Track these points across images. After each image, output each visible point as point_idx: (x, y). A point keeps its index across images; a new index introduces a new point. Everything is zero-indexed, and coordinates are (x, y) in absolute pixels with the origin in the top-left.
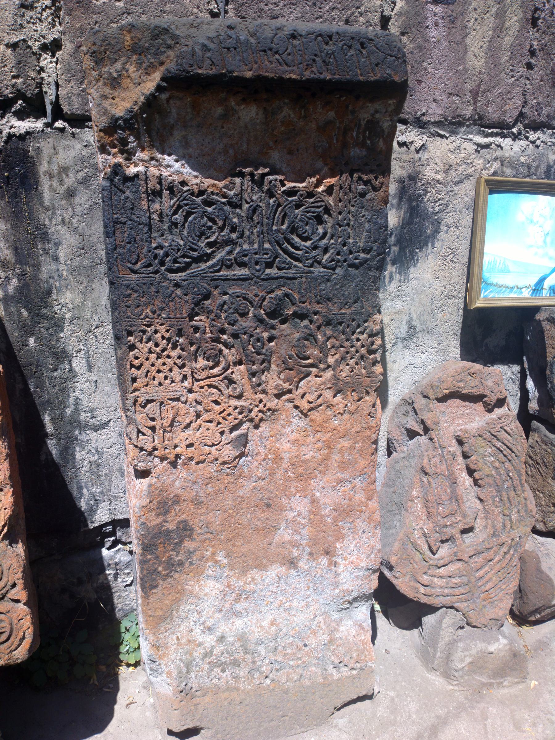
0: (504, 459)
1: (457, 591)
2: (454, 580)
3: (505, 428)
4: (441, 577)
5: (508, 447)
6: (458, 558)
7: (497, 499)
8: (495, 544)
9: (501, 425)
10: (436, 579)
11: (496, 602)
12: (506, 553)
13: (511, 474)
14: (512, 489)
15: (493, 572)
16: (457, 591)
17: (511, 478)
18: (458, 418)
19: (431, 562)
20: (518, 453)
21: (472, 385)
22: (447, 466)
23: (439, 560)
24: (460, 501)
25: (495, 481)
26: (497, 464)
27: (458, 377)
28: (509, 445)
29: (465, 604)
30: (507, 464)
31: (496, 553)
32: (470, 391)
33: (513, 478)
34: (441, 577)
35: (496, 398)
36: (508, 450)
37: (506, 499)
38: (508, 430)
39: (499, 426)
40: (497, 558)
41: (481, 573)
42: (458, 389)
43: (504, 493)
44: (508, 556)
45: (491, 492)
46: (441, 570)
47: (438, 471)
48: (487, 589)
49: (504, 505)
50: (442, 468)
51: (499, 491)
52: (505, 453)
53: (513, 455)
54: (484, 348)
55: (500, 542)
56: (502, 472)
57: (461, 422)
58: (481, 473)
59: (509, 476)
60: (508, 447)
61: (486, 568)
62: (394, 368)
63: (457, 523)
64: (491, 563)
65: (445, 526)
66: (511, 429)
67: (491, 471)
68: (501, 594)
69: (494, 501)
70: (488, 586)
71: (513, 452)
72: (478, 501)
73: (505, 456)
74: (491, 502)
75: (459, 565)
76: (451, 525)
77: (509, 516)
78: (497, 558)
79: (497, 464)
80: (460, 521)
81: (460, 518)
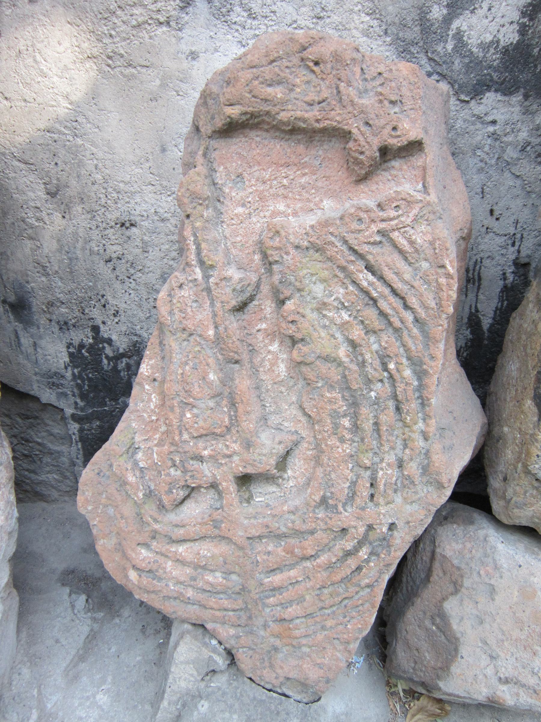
0: (377, 323)
1: (212, 602)
2: (210, 578)
3: (395, 235)
4: (180, 561)
5: (394, 292)
6: (222, 534)
7: (346, 422)
8: (322, 525)
9: (383, 225)
10: (170, 563)
11: (306, 649)
12: (348, 554)
13: (392, 366)
14: (391, 404)
15: (309, 585)
16: (212, 602)
17: (391, 377)
18: (276, 196)
19: (157, 526)
20: (422, 314)
21: (312, 96)
22: (215, 315)
23: (177, 526)
24: (241, 408)
25: (345, 376)
26: (357, 333)
27: (268, 72)
28: (399, 285)
29: (232, 631)
30: (387, 337)
31: (326, 548)
32: (299, 114)
33: (397, 376)
34: (180, 561)
35: (376, 142)
36: (392, 299)
37: (368, 426)
38: (403, 242)
39: (374, 228)
40: (323, 559)
41: (277, 579)
42: (266, 108)
43: (365, 410)
44: (352, 562)
45: (330, 401)
46: (181, 549)
47: (189, 324)
48: (286, 616)
49: (362, 440)
50: (199, 317)
51: (355, 404)
52: (383, 305)
53: (409, 317)
54: (450, 47)
55: (337, 523)
56: (368, 356)
57: (281, 207)
58: (305, 349)
59: (386, 369)
60: (394, 292)
61: (292, 573)
62: (194, 73)
63: (230, 456)
64: (308, 564)
65: (200, 459)
66: (412, 243)
67: (336, 347)
68: (320, 636)
69: (336, 426)
70: (292, 611)
71: (406, 307)
72: (303, 419)
73: (382, 314)
74: (329, 427)
75: (224, 548)
76: (211, 456)
77: (373, 469)
78: (323, 559)
79: (357, 333)
80: (235, 453)
81: (236, 447)
